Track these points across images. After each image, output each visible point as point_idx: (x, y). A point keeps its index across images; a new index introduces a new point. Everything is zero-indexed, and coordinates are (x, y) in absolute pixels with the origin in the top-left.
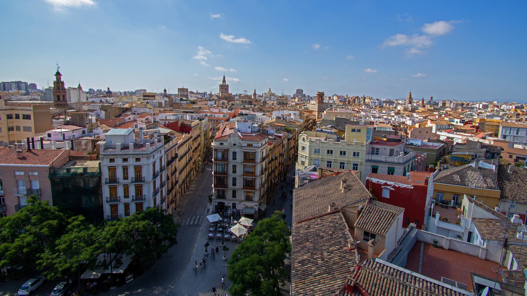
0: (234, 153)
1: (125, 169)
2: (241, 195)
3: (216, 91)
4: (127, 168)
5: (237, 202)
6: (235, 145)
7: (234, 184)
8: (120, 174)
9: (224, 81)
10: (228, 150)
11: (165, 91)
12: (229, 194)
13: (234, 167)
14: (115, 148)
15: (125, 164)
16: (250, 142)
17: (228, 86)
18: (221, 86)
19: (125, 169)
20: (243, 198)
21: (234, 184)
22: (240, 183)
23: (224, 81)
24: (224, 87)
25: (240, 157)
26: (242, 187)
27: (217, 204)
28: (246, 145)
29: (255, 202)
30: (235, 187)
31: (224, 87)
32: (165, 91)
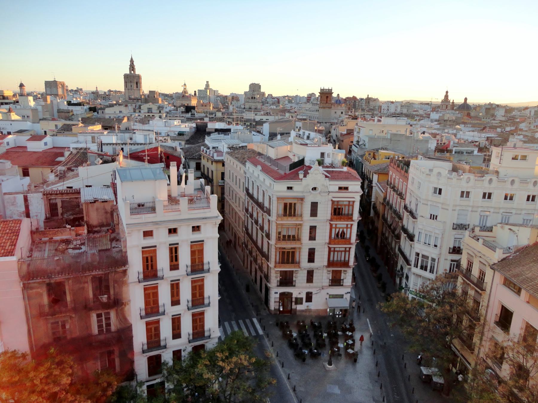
0: (314, 206)
1: (174, 251)
2: (323, 277)
3: (119, 86)
4: (176, 249)
5: (314, 291)
6: (314, 189)
7: (311, 259)
8: (163, 261)
9: (132, 67)
10: (302, 199)
11: (21, 86)
12: (300, 277)
13: (313, 229)
14: (153, 209)
15: (173, 239)
16: (343, 184)
17: (139, 77)
18: (126, 77)
19: (174, 251)
20: (326, 282)
21: (311, 259)
22: (321, 258)
23: (132, 67)
24: (132, 80)
25: (325, 212)
26: (326, 263)
27: (278, 296)
28: (337, 189)
29: (347, 287)
30: (311, 265)
31: (132, 80)
32: (21, 86)
